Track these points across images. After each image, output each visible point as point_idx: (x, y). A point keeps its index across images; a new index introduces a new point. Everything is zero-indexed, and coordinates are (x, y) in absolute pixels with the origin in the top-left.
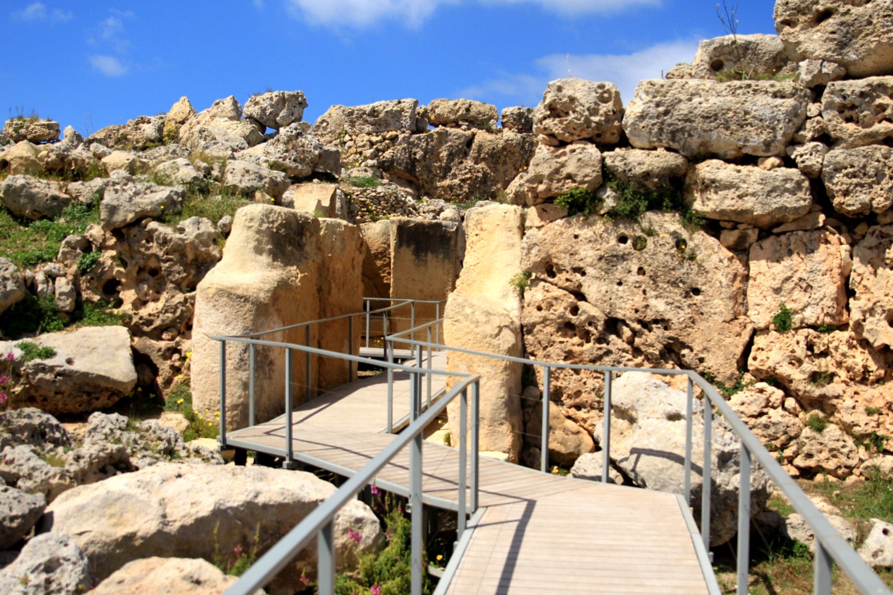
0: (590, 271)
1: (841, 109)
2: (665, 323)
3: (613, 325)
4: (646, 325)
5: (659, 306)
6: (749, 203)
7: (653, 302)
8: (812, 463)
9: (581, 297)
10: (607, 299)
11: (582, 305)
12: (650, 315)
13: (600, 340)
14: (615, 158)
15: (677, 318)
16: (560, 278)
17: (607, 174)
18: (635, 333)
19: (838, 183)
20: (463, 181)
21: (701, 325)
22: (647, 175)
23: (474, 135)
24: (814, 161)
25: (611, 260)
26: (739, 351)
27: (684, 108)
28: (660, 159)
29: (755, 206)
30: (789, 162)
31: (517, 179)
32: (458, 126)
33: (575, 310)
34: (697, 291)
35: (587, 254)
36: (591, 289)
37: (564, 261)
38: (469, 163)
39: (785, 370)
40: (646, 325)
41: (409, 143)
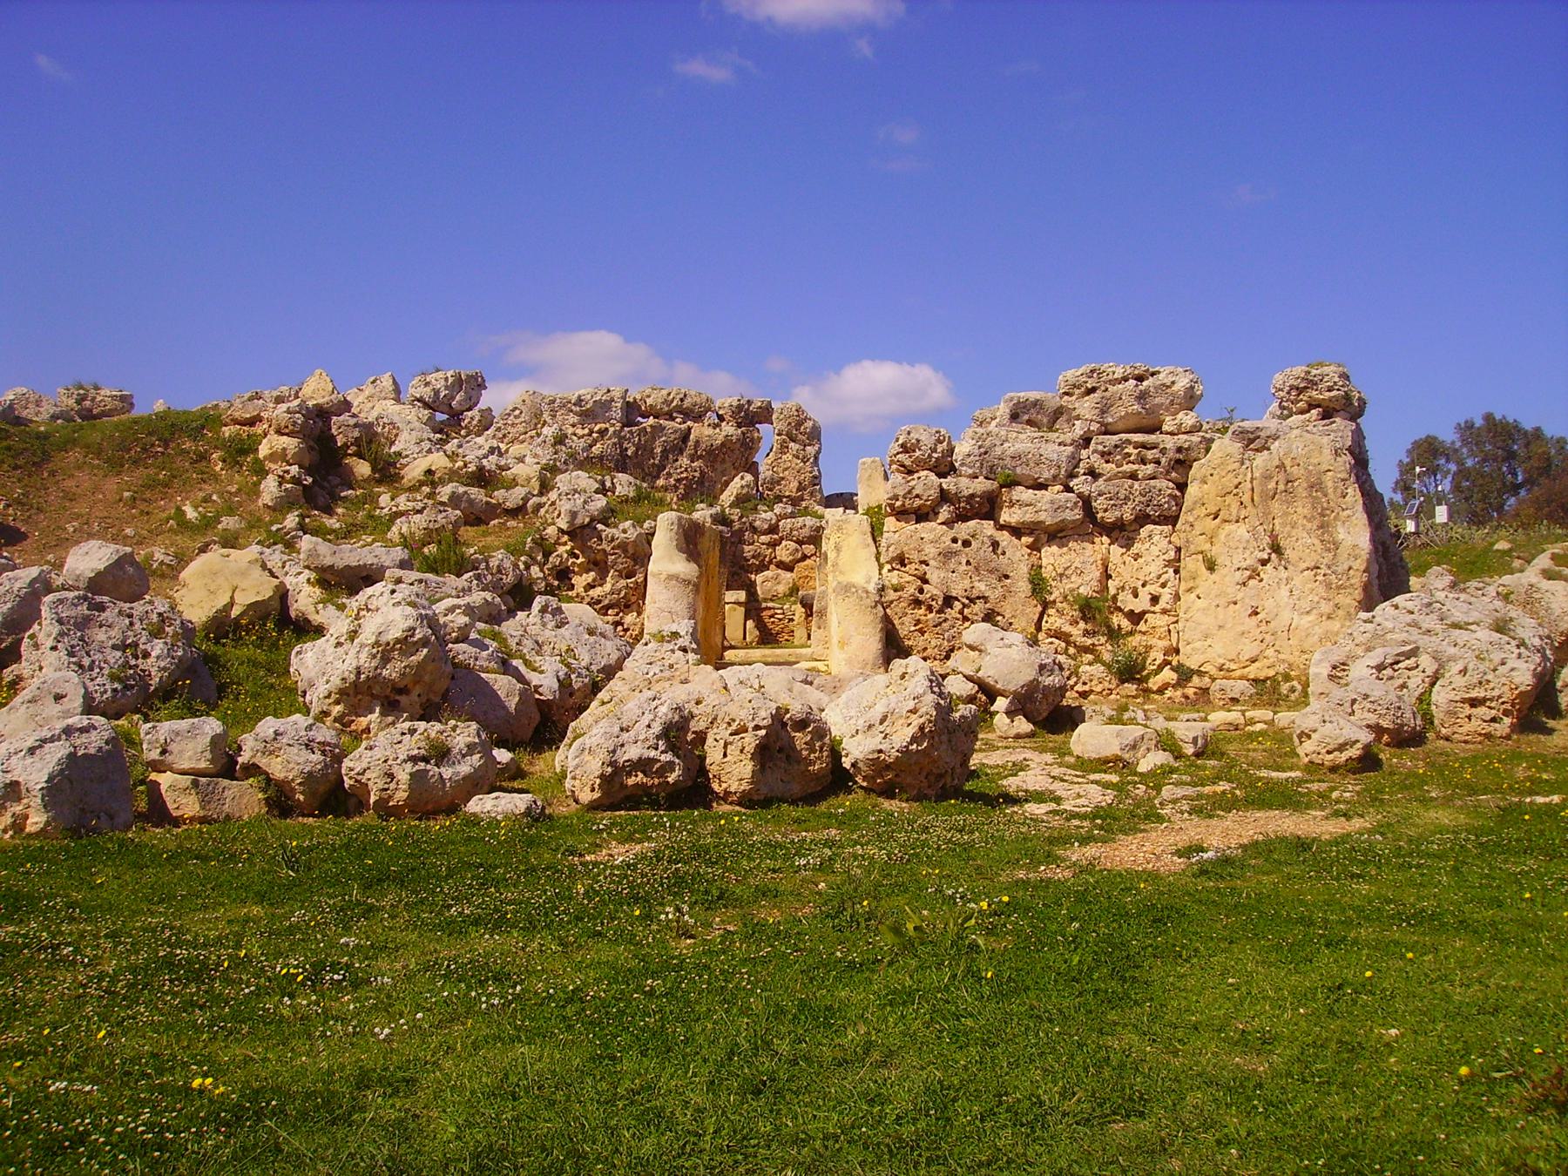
0: (932, 562)
1: (1103, 454)
2: (985, 599)
3: (949, 601)
4: (972, 601)
5: (981, 587)
6: (1042, 516)
7: (976, 584)
8: (1086, 688)
9: (926, 582)
10: (944, 582)
11: (926, 587)
12: (975, 593)
13: (939, 612)
14: (948, 483)
15: (993, 595)
16: (910, 568)
17: (944, 497)
18: (964, 606)
19: (1100, 504)
20: (678, 481)
21: (1010, 600)
22: (972, 496)
23: (690, 429)
24: (1085, 489)
25: (947, 555)
26: (1036, 617)
27: (998, 450)
28: (981, 485)
29: (1047, 518)
30: (1068, 489)
31: (737, 479)
32: (673, 419)
33: (921, 591)
34: (1007, 577)
35: (930, 551)
36: (934, 575)
37: (915, 556)
38: (684, 461)
39: (1067, 628)
40: (972, 601)
41: (620, 438)
